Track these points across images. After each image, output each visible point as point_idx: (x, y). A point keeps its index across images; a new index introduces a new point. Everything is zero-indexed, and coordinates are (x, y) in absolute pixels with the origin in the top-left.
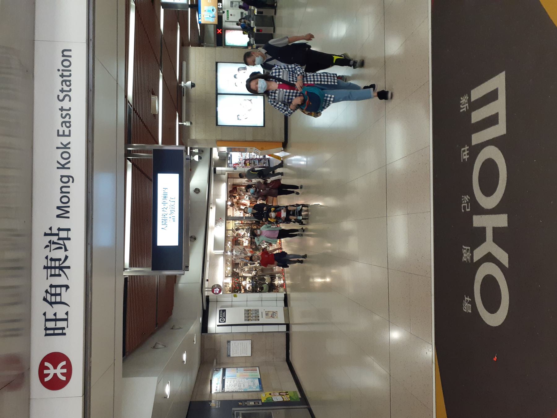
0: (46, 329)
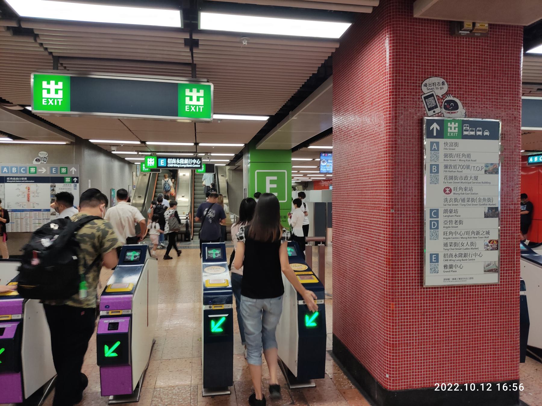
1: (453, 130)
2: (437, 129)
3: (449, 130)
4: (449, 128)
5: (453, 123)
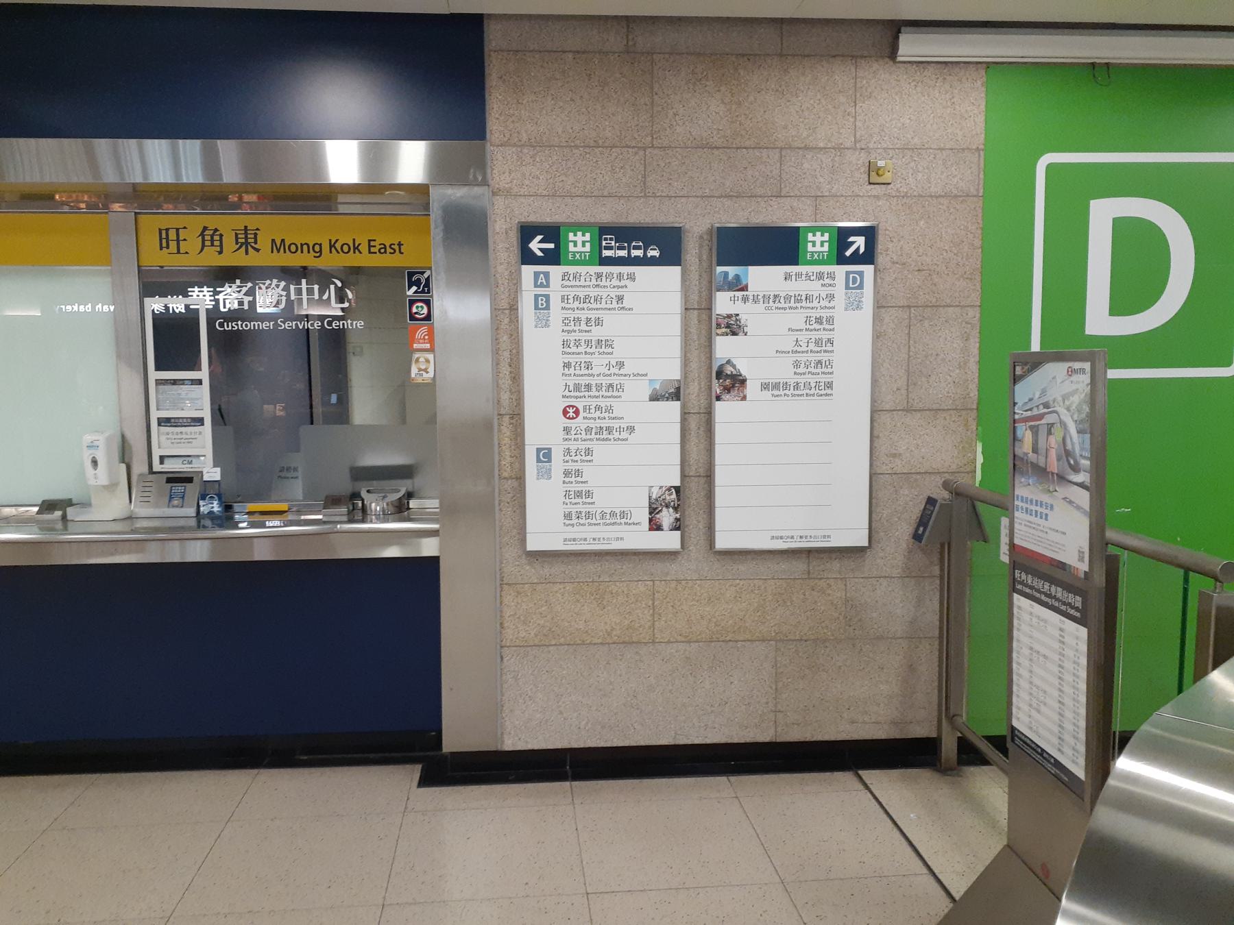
0: (167, 230)
1: (579, 248)
3: (571, 248)
4: (571, 245)
5: (579, 234)
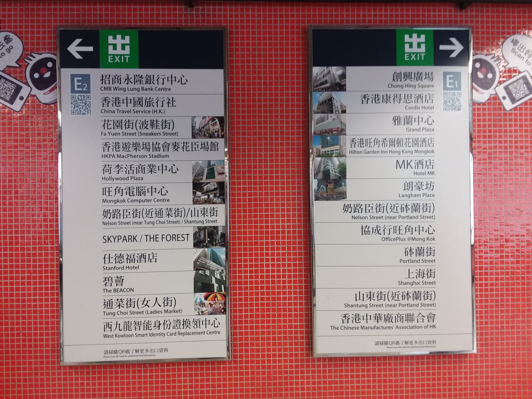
1: (119, 51)
2: (79, 45)
4: (110, 48)
